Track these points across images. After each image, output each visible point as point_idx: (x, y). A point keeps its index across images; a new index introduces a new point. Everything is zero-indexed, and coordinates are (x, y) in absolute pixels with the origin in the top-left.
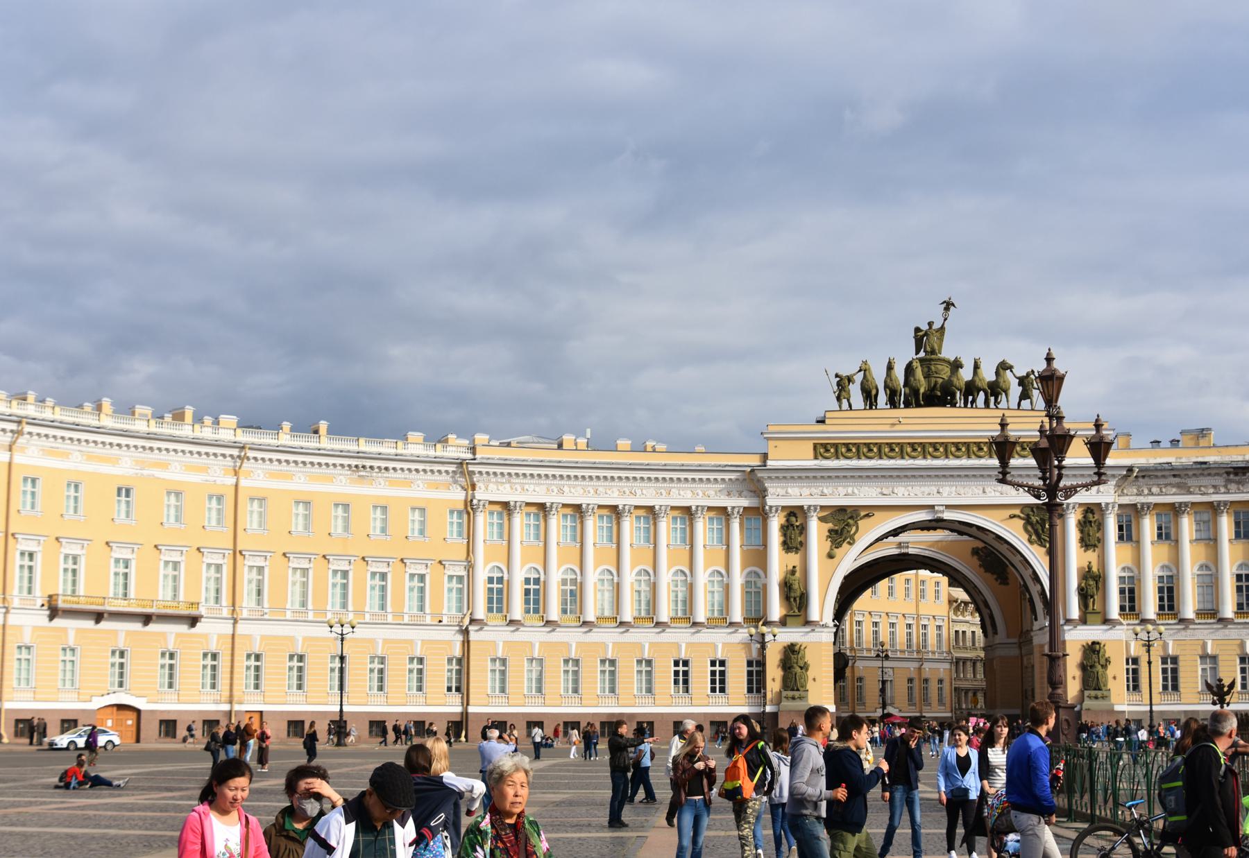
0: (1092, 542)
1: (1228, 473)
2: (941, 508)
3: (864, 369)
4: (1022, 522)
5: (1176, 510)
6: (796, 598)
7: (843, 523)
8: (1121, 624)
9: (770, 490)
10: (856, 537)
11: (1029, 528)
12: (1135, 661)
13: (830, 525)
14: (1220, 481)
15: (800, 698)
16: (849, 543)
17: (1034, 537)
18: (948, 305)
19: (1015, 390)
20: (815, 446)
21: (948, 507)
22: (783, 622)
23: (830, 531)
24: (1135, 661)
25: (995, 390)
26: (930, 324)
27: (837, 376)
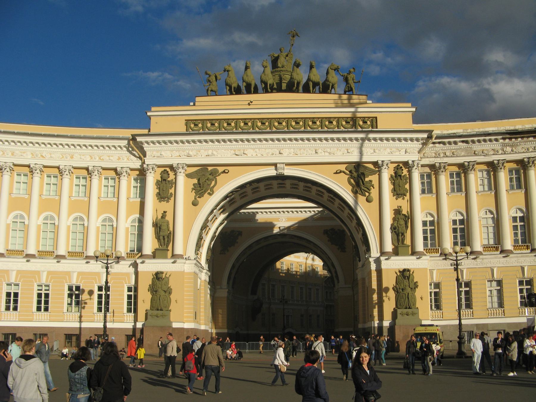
0: (402, 192)
1: (504, 139)
2: (282, 166)
5: (464, 169)
6: (165, 235)
7: (204, 178)
8: (425, 255)
9: (148, 154)
10: (214, 189)
11: (352, 181)
12: (437, 285)
13: (195, 181)
14: (497, 146)
15: (163, 316)
16: (210, 194)
22: (154, 256)
23: (194, 185)
24: (437, 285)
27: (206, 74)
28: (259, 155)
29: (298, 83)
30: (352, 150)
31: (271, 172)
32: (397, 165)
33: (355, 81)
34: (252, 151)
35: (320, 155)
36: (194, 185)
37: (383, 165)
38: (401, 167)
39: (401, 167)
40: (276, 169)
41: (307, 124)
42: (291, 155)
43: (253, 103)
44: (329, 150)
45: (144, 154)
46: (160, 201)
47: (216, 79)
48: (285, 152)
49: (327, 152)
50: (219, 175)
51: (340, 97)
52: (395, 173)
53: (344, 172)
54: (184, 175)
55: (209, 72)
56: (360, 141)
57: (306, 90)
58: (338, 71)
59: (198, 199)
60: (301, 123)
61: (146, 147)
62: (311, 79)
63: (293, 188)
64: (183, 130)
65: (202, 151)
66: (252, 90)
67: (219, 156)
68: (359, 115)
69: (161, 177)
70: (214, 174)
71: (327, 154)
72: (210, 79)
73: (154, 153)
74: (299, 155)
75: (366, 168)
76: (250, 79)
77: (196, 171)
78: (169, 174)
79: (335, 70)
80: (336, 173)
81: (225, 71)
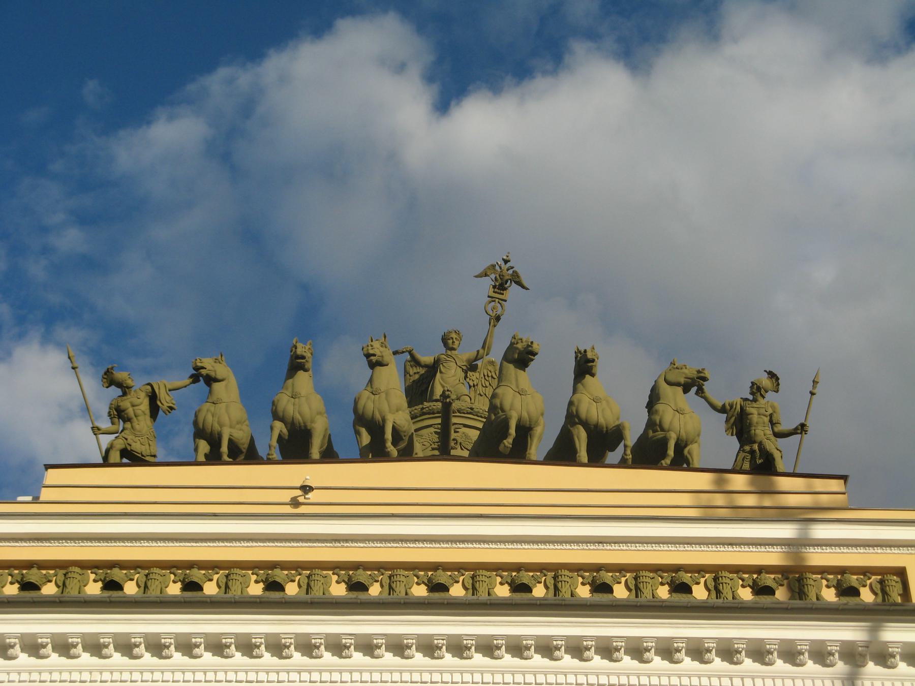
29: (525, 431)
33: (778, 429)
47: (154, 410)
51: (719, 482)
55: (120, 375)
56: (841, 667)
57: (563, 454)
58: (700, 392)
62: (583, 415)
68: (817, 558)
72: (125, 404)
79: (686, 389)
81: (195, 378)
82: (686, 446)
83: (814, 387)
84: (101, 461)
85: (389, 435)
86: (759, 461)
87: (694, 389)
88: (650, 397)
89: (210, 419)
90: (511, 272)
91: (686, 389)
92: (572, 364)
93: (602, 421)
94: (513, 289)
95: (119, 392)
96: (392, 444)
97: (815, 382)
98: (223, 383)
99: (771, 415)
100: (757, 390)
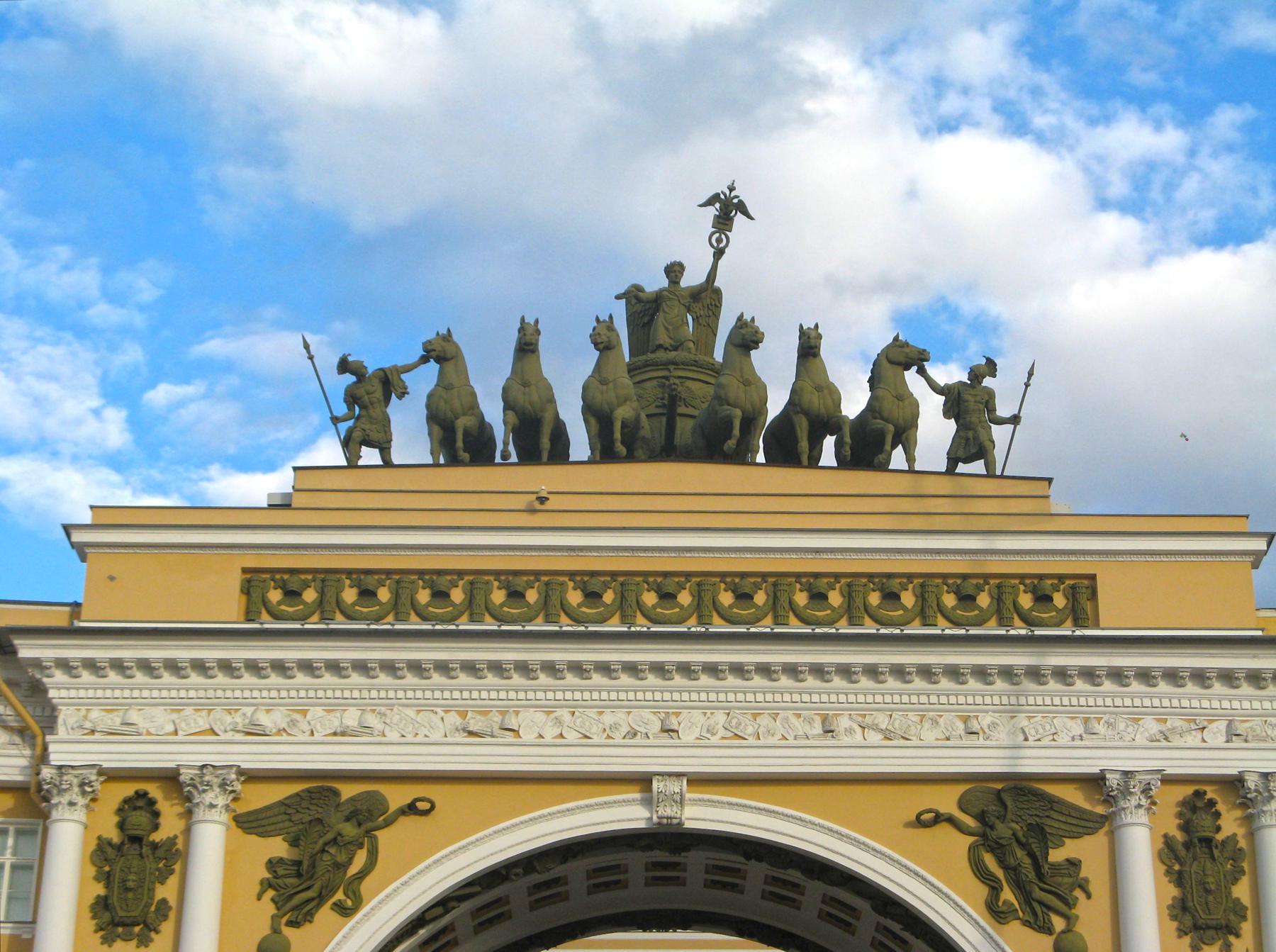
0: (1219, 916)
2: (674, 786)
3: (441, 352)
4: (971, 840)
9: (67, 717)
10: (365, 886)
11: (990, 861)
13: (278, 847)
16: (345, 911)
17: (1008, 895)
18: (727, 209)
19: (935, 431)
20: (253, 582)
21: (699, 781)
23: (272, 864)
25: (871, 442)
26: (674, 271)
28: (572, 737)
30: (986, 720)
31: (626, 814)
32: (1189, 790)
34: (540, 717)
35: (846, 740)
36: (272, 864)
37: (1126, 792)
38: (1212, 803)
39: (1212, 803)
40: (648, 802)
41: (783, 599)
42: (715, 740)
43: (549, 505)
44: (883, 721)
45: (49, 722)
46: (108, 940)
48: (691, 725)
49: (875, 728)
50: (388, 824)
52: (1186, 828)
53: (951, 820)
54: (225, 817)
59: (288, 932)
60: (760, 598)
61: (58, 687)
63: (715, 884)
64: (229, 612)
65: (316, 712)
66: (545, 443)
67: (393, 736)
69: (121, 826)
70: (368, 816)
71: (874, 738)
73: (95, 714)
74: (752, 741)
75: (1052, 802)
76: (535, 397)
77: (281, 803)
78: (156, 814)
80: (919, 822)
81: (424, 360)
82: (904, 431)
83: (1029, 379)
84: (345, 463)
85: (618, 435)
86: (973, 451)
87: (915, 368)
88: (872, 371)
89: (442, 404)
90: (735, 201)
91: (907, 368)
92: (795, 342)
93: (823, 411)
94: (739, 219)
95: (354, 379)
96: (622, 443)
97: (1030, 374)
98: (452, 362)
99: (987, 402)
100: (976, 375)
